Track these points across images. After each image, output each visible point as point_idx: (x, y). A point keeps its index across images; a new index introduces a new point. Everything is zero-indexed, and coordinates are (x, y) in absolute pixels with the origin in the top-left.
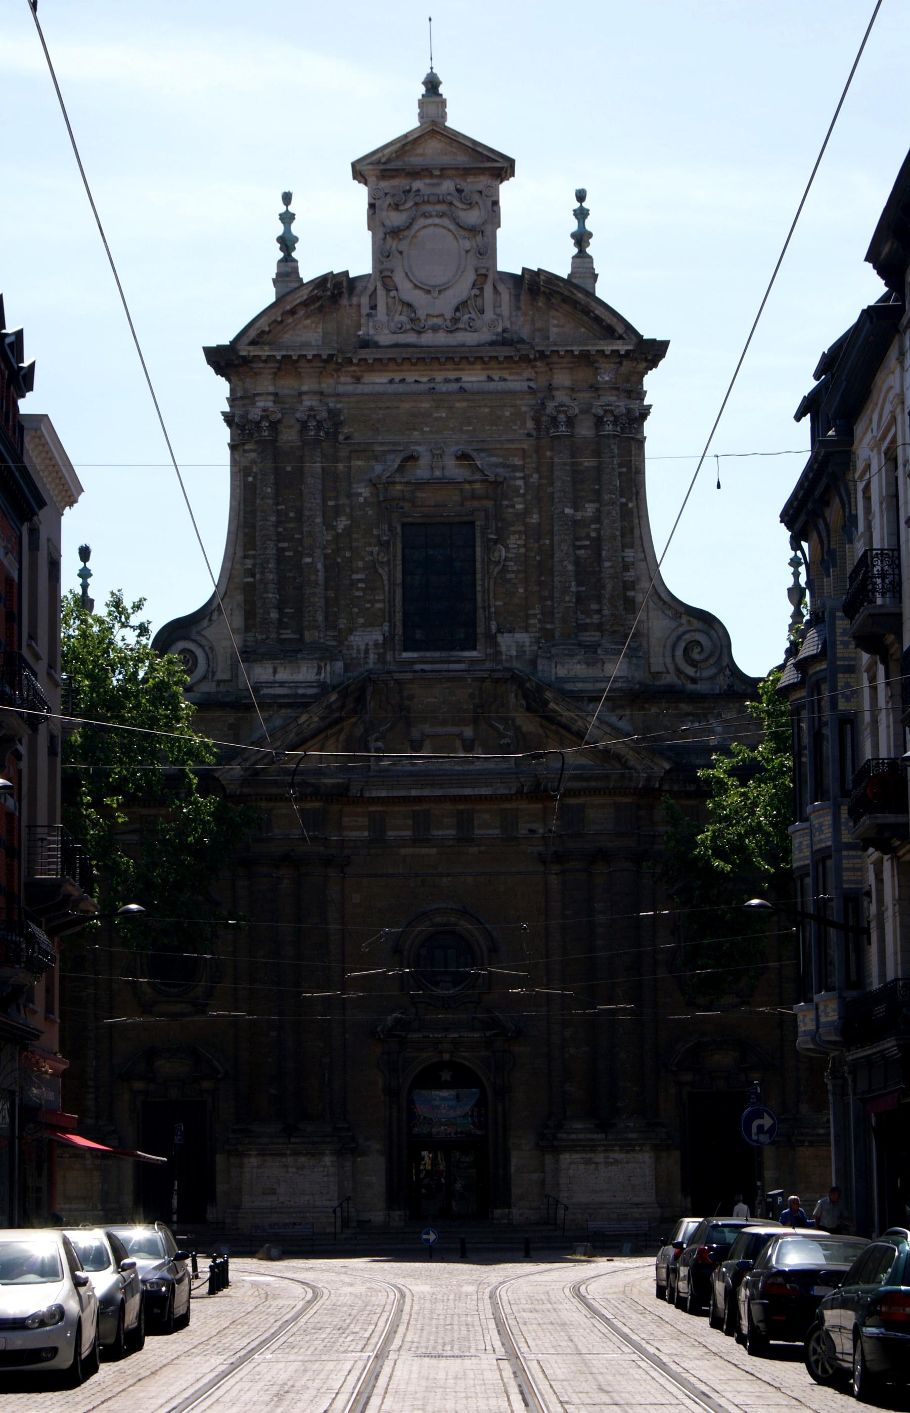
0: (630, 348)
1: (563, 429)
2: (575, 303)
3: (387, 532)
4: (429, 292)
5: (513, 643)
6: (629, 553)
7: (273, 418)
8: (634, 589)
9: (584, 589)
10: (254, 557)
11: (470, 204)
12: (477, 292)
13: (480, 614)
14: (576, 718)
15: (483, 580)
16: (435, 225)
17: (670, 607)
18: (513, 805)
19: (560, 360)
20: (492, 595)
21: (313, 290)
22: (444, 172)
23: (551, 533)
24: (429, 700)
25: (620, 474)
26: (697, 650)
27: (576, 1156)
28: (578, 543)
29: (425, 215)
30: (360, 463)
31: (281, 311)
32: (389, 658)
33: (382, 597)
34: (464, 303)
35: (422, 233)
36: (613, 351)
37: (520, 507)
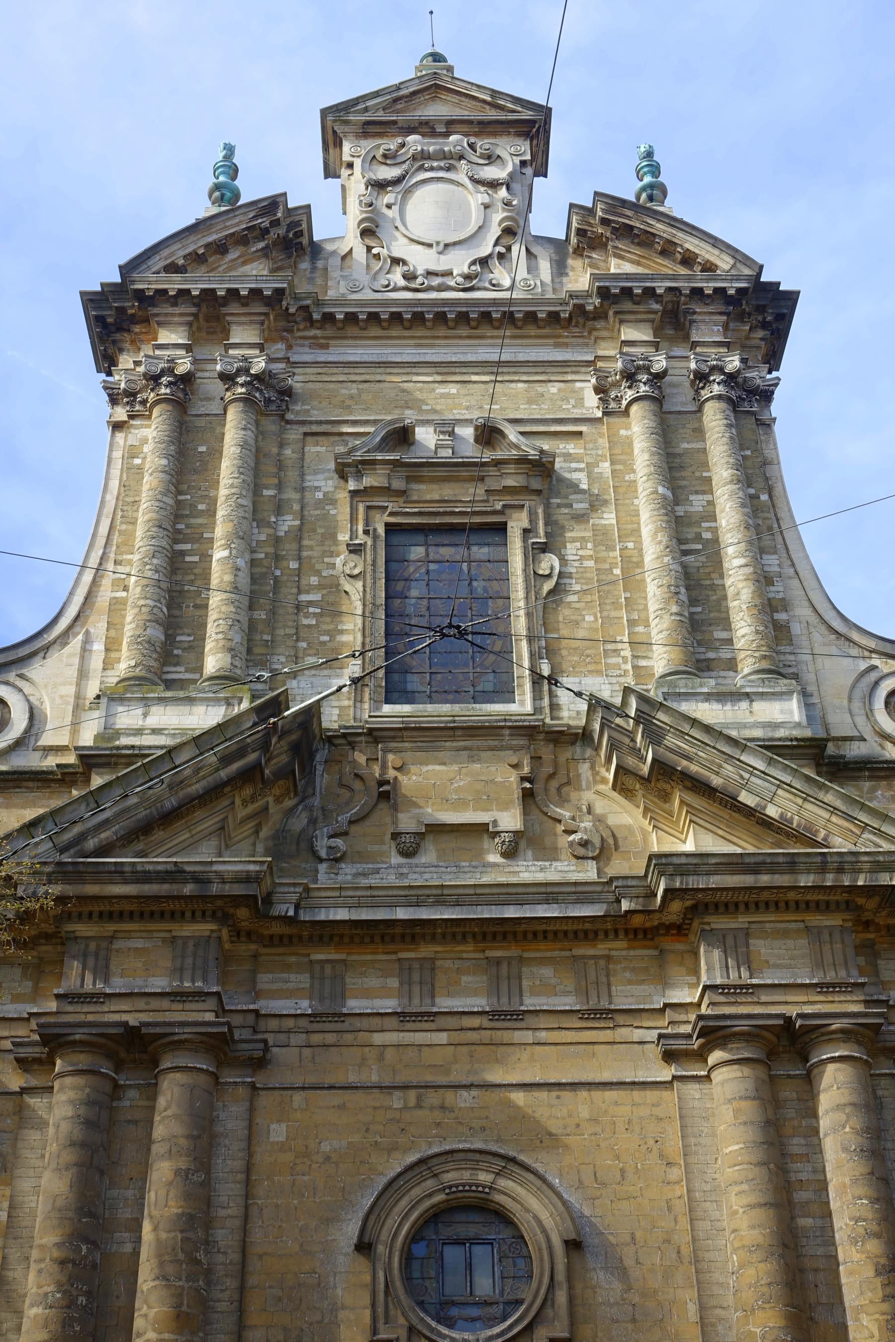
4: (430, 246)
9: (699, 609)
11: (489, 157)
12: (503, 250)
16: (439, 179)
19: (635, 308)
21: (255, 217)
22: (451, 125)
28: (683, 547)
30: (318, 449)
34: (484, 262)
36: (716, 290)
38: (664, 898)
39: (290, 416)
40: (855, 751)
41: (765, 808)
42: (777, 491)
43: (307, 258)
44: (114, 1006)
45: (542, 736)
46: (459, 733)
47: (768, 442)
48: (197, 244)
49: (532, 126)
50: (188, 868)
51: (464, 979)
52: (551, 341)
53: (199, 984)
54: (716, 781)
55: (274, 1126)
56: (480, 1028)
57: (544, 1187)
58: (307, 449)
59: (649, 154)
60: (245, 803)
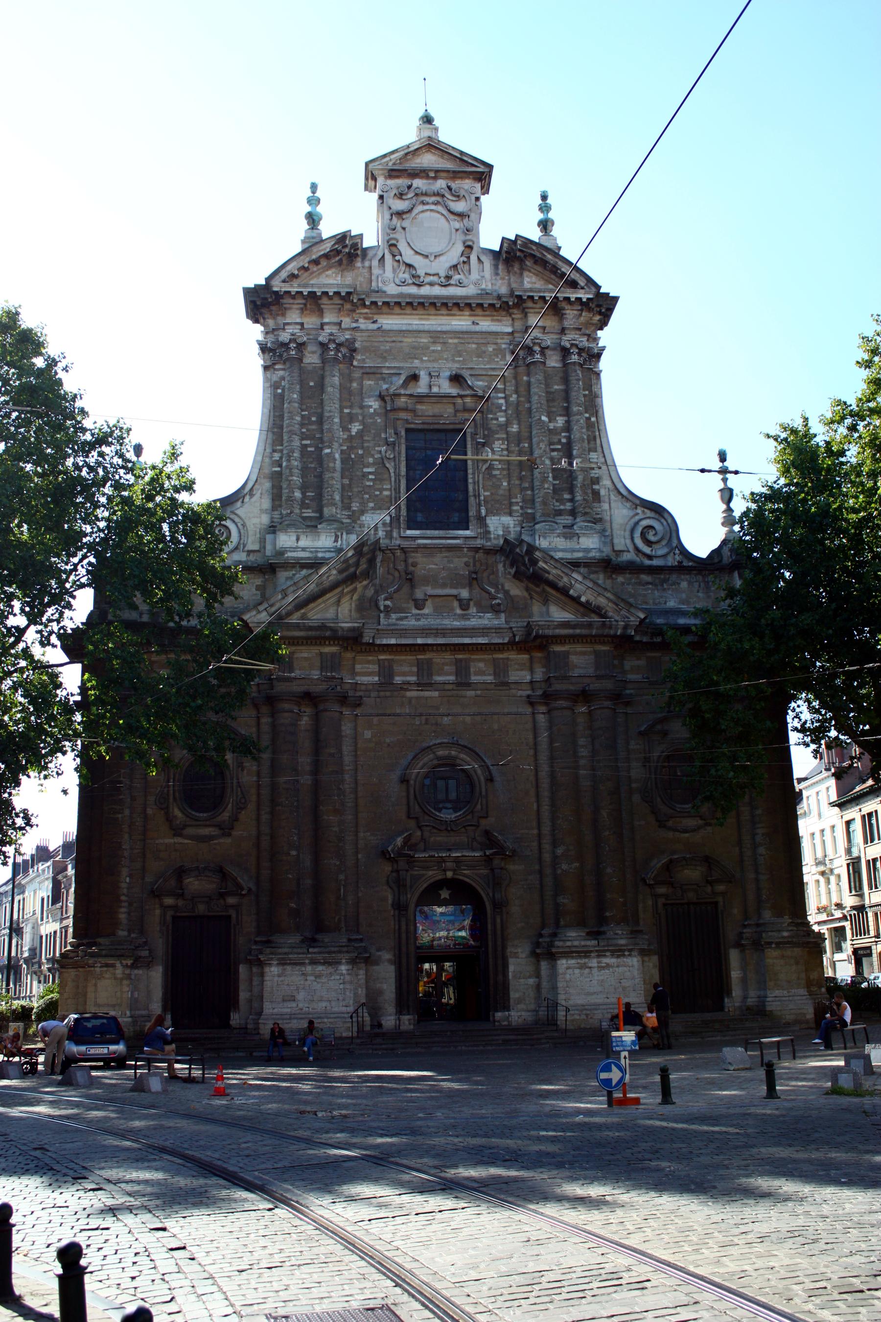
0: (591, 296)
1: (538, 356)
2: (543, 263)
3: (393, 436)
4: (427, 257)
5: (501, 525)
6: (593, 455)
7: (300, 341)
8: (598, 483)
10: (281, 451)
11: (458, 196)
12: (465, 260)
13: (472, 500)
15: (473, 474)
16: (431, 210)
17: (627, 500)
19: (534, 306)
20: (481, 486)
22: (438, 173)
23: (530, 438)
24: (431, 566)
25: (585, 396)
26: (652, 533)
27: (572, 962)
28: (552, 447)
29: (423, 203)
30: (370, 382)
31: (308, 259)
32: (395, 534)
33: (388, 487)
34: (455, 267)
35: (421, 215)
36: (576, 298)
37: (502, 419)
43: (359, 259)
47: (597, 384)
49: (482, 174)
50: (328, 625)
51: (446, 668)
52: (489, 318)
54: (561, 584)
55: (366, 732)
56: (453, 690)
58: (364, 382)
59: (544, 197)
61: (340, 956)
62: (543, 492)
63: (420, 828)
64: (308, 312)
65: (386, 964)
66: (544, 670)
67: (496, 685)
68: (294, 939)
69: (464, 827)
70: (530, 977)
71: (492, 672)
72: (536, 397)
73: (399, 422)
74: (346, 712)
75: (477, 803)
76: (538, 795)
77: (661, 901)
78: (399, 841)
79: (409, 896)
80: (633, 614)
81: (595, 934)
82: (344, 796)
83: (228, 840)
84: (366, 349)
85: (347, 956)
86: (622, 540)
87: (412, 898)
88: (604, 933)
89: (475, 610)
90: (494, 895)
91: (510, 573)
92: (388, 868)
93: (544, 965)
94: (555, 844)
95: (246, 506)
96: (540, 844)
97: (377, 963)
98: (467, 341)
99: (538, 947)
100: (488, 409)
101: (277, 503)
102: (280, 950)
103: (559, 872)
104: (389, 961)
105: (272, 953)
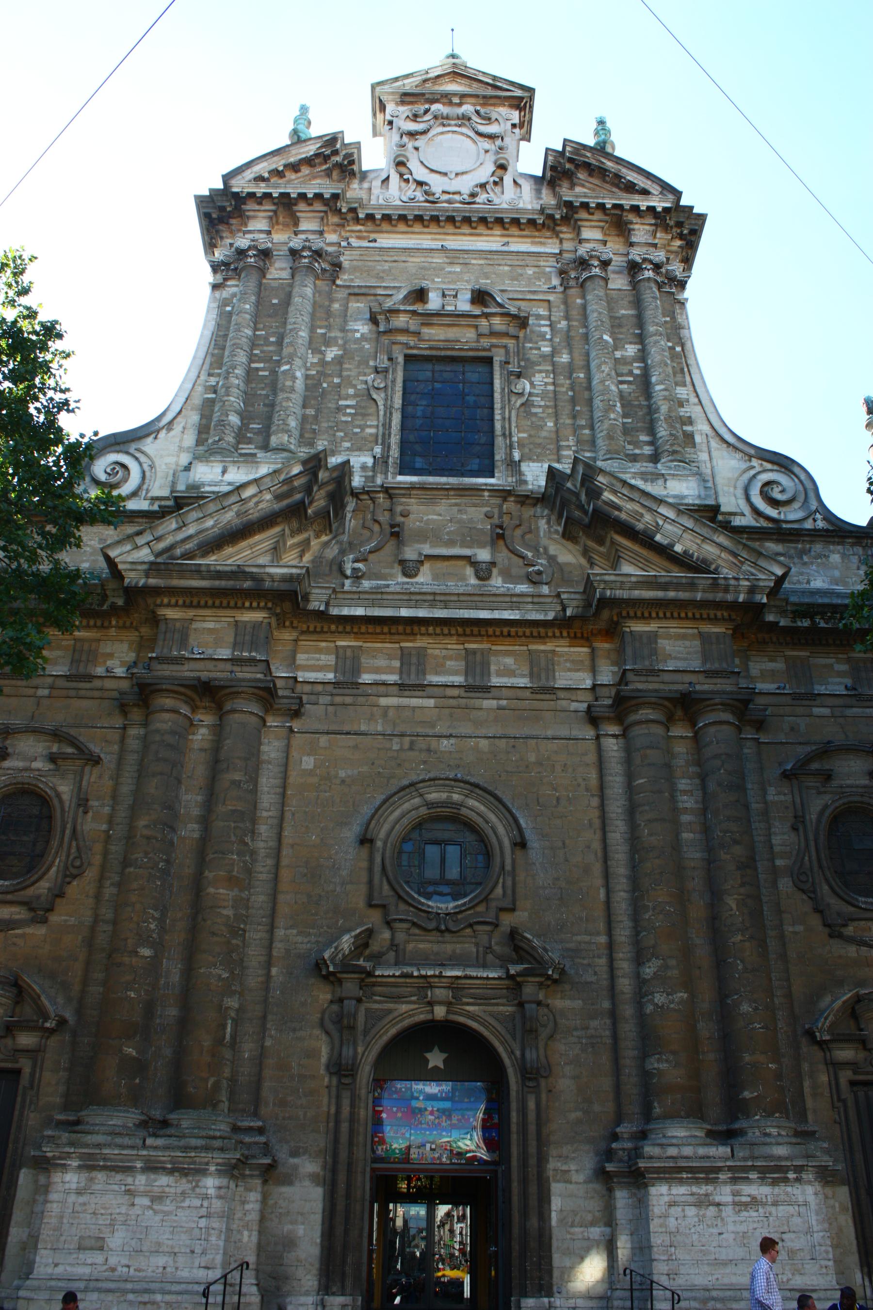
0: (668, 205)
1: (597, 270)
4: (445, 174)
7: (262, 247)
9: (630, 420)
10: (219, 375)
13: (499, 441)
14: (641, 510)
15: (503, 408)
17: (736, 448)
18: (548, 646)
19: (590, 217)
20: (513, 425)
23: (587, 368)
24: (430, 517)
27: (680, 1190)
29: (444, 125)
30: (359, 305)
31: (283, 162)
33: (375, 423)
34: (483, 186)
37: (546, 349)
38: (597, 606)
39: (338, 282)
40: (737, 521)
41: (673, 546)
42: (688, 346)
44: (192, 665)
45: (512, 499)
46: (452, 493)
47: (682, 314)
48: (278, 163)
49: (522, 100)
50: (247, 569)
51: (448, 663)
52: (529, 240)
53: (254, 654)
54: (640, 526)
55: (305, 758)
56: (459, 697)
57: (500, 806)
60: (293, 534)
61: (205, 1156)
62: (606, 425)
63: (388, 924)
64: (281, 227)
65: (307, 1183)
66: (616, 669)
67: (533, 690)
68: (124, 1118)
69: (471, 925)
70: (592, 1224)
71: (527, 672)
72: (595, 315)
73: (395, 347)
74: (271, 721)
75: (497, 883)
76: (607, 875)
77: (845, 1076)
78: (346, 942)
79: (360, 1050)
80: (762, 569)
81: (726, 1136)
82: (254, 861)
83: (40, 931)
84: (355, 269)
85: (219, 1157)
86: (733, 499)
87: (366, 1056)
88: (741, 1133)
89: (500, 580)
90: (523, 1055)
91: (557, 532)
92: (324, 995)
93: (622, 1197)
94: (639, 960)
95: (158, 441)
96: (611, 960)
97: (288, 1180)
98: (496, 262)
99: (609, 1160)
100: (525, 337)
101: (204, 436)
102: (89, 1139)
103: (649, 1009)
104: (314, 1178)
105: (72, 1144)
